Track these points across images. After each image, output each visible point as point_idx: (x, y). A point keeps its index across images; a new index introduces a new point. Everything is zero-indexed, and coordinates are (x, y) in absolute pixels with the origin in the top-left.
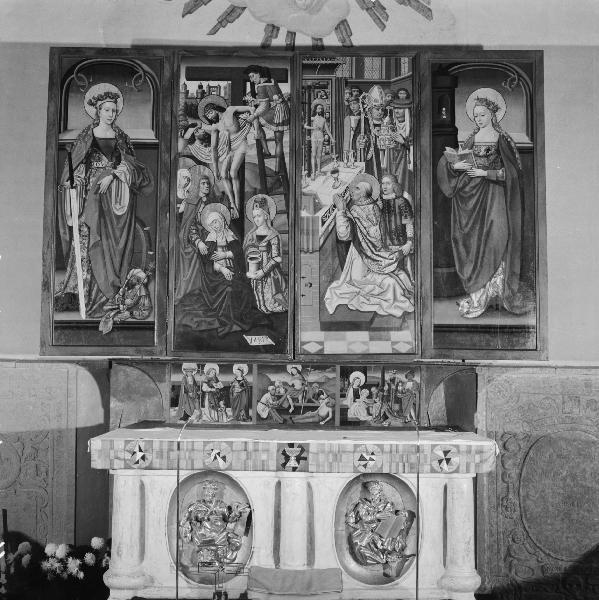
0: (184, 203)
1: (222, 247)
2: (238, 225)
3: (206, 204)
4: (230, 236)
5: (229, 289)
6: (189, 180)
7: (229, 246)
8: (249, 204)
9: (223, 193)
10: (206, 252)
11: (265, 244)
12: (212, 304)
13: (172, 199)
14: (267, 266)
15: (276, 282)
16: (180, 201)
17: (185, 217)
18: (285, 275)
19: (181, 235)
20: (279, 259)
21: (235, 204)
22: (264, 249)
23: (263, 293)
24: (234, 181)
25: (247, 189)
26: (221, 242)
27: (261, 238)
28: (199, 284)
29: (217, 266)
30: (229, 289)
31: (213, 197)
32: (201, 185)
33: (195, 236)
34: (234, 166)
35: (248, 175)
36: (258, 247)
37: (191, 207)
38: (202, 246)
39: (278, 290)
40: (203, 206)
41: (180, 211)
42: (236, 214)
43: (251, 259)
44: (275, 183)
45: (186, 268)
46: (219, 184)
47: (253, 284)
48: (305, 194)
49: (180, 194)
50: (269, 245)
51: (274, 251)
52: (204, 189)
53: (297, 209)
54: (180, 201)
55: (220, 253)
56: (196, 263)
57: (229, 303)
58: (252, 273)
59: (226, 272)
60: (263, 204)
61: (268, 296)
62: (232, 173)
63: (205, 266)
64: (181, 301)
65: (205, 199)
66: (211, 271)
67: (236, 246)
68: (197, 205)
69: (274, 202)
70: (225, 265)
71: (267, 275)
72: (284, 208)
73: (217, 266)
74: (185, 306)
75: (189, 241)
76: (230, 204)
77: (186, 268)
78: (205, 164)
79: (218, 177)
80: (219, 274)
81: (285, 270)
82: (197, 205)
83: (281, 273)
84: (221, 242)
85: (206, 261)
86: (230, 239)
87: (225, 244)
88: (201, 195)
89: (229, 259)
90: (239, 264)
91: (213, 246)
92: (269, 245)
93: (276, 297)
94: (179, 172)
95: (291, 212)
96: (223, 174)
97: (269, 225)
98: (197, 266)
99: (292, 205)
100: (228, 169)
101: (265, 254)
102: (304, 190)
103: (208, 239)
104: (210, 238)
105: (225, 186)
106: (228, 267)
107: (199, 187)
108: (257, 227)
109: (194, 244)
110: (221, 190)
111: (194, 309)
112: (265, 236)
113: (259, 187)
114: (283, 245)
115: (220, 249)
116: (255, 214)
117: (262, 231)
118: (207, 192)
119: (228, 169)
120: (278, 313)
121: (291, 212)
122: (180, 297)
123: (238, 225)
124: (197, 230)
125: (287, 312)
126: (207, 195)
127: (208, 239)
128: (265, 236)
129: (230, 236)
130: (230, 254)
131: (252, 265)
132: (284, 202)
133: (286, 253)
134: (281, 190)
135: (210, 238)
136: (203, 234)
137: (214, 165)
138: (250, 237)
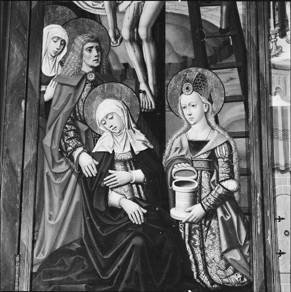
0: (53, 83)
1: (124, 162)
2: (154, 122)
3: (94, 84)
4: (139, 142)
5: (137, 241)
6: (63, 43)
7: (136, 161)
8: (172, 84)
9: (126, 65)
10: (94, 172)
11: (206, 156)
12: (105, 271)
13: (31, 77)
14: (210, 199)
15: (228, 226)
16: (45, 80)
17: (54, 108)
18: (246, 215)
19: (47, 141)
20: (231, 185)
21: (147, 87)
22: (203, 165)
23: (203, 248)
24: (145, 46)
25: (169, 59)
26: (122, 152)
27: (196, 146)
28: (79, 232)
29: (114, 198)
30: (137, 241)
31: (109, 76)
32: (86, 53)
33: (72, 143)
34: (144, 20)
35: (170, 34)
36: (191, 162)
37: (66, 91)
38: (87, 163)
39: (233, 243)
40: (88, 87)
41: (47, 97)
42: (148, 101)
43: (180, 184)
44: (220, 48)
45: (56, 199)
46: (118, 50)
47: (185, 232)
48: (275, 67)
49: (47, 68)
50: (212, 158)
51: (222, 168)
52: (91, 59)
53: (264, 93)
54: (45, 80)
55: (120, 175)
56: (75, 195)
57: (138, 268)
58: (183, 210)
59: (134, 211)
60: (199, 85)
61: (213, 254)
62: (142, 32)
63: (91, 200)
64: (45, 263)
65: (91, 77)
66: (103, 208)
67: (151, 162)
68: (77, 87)
69: (228, 80)
70: (128, 195)
71: (210, 214)
72: (239, 92)
73: (114, 198)
74: (51, 275)
75: (61, 153)
76: (138, 84)
77: (56, 199)
78: (94, 17)
79: (116, 38)
80: (119, 211)
81: (244, 204)
82: (77, 87)
83: (238, 210)
84: (122, 152)
85: (94, 189)
86: (139, 147)
87: (129, 156)
88: (86, 69)
89: (137, 183)
90: (157, 192)
91: (107, 161)
92: (212, 158)
93: (229, 256)
94: (46, 30)
95: (253, 101)
96: (125, 33)
97: (212, 120)
98: (76, 198)
99: (253, 86)
100: (135, 24)
101: (205, 175)
102: (274, 60)
103: (99, 147)
104: (102, 146)
105: (130, 54)
106: (134, 200)
107: (82, 56)
108: (190, 126)
109: (71, 157)
110: (122, 61)
111: (70, 281)
112: (205, 143)
113: (191, 55)
114: (240, 159)
115: (118, 166)
116: (190, 103)
117: (198, 132)
118: (96, 65)
119: (135, 24)
120: (233, 288)
121: (253, 101)
122: (42, 257)
123: (154, 122)
124: (77, 131)
125: (250, 284)
126: (96, 70)
127: (99, 147)
128: (205, 143)
129: (139, 142)
130: (138, 175)
131: (182, 196)
132: (238, 81)
133: (246, 173)
134: (233, 59)
135: (102, 146)
136: (89, 137)
137: (110, 18)
138: (176, 144)
